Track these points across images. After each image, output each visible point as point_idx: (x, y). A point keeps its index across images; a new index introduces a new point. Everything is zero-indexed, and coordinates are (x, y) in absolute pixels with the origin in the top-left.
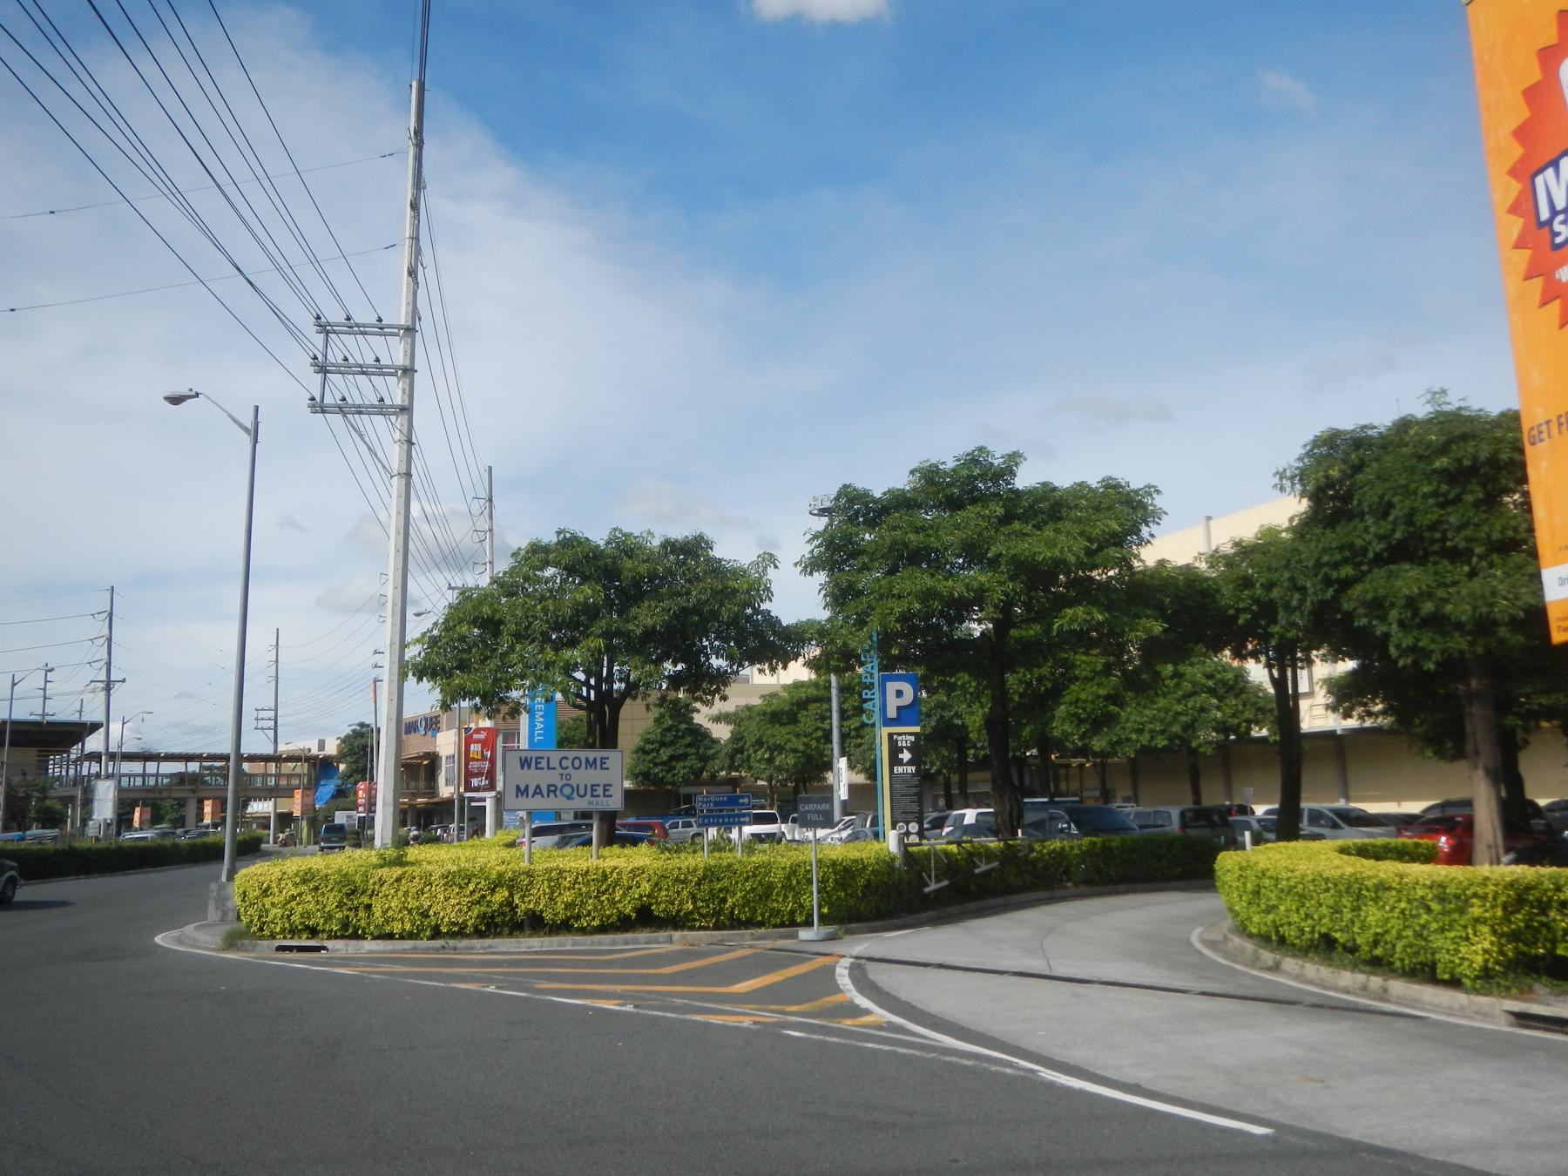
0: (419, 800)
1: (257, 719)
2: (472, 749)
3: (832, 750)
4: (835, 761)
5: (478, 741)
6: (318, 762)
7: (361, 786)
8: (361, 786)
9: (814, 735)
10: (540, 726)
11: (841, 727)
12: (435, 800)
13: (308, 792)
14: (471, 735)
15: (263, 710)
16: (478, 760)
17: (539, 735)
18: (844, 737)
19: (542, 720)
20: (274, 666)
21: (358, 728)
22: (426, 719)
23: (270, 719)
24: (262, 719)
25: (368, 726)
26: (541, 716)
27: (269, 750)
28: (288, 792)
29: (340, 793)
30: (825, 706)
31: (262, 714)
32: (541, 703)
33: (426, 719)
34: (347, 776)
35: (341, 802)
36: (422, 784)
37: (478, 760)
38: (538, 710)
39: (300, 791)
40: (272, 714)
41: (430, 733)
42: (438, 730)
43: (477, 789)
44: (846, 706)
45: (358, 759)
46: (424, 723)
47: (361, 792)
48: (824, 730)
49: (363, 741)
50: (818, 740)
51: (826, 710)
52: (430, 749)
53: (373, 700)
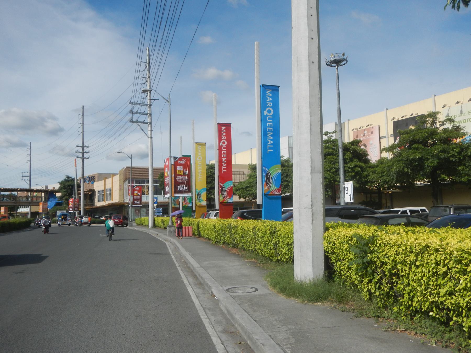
0: (87, 207)
1: (22, 176)
2: (178, 169)
3: (340, 178)
4: (341, 183)
5: (181, 165)
6: (48, 192)
7: (71, 200)
8: (71, 200)
9: (332, 171)
10: (270, 142)
11: (344, 167)
12: (94, 207)
13: (45, 204)
14: (177, 161)
15: (25, 173)
16: (181, 175)
17: (270, 148)
18: (345, 172)
19: (272, 138)
20: (29, 157)
21: (67, 178)
22: (89, 178)
23: (28, 176)
24: (25, 176)
25: (71, 177)
26: (271, 135)
27: (27, 187)
28: (37, 204)
29: (58, 204)
30: (335, 157)
31: (24, 175)
32: (271, 127)
33: (89, 178)
34: (61, 198)
35: (59, 207)
36: (88, 201)
37: (181, 175)
38: (269, 131)
39: (42, 203)
40: (29, 174)
41: (91, 183)
42: (94, 181)
43: (181, 192)
44: (346, 157)
45: (67, 190)
46: (88, 179)
47: (70, 203)
48: (335, 168)
49: (69, 183)
50: (333, 173)
51: (336, 159)
52: (92, 188)
53: (75, 166)
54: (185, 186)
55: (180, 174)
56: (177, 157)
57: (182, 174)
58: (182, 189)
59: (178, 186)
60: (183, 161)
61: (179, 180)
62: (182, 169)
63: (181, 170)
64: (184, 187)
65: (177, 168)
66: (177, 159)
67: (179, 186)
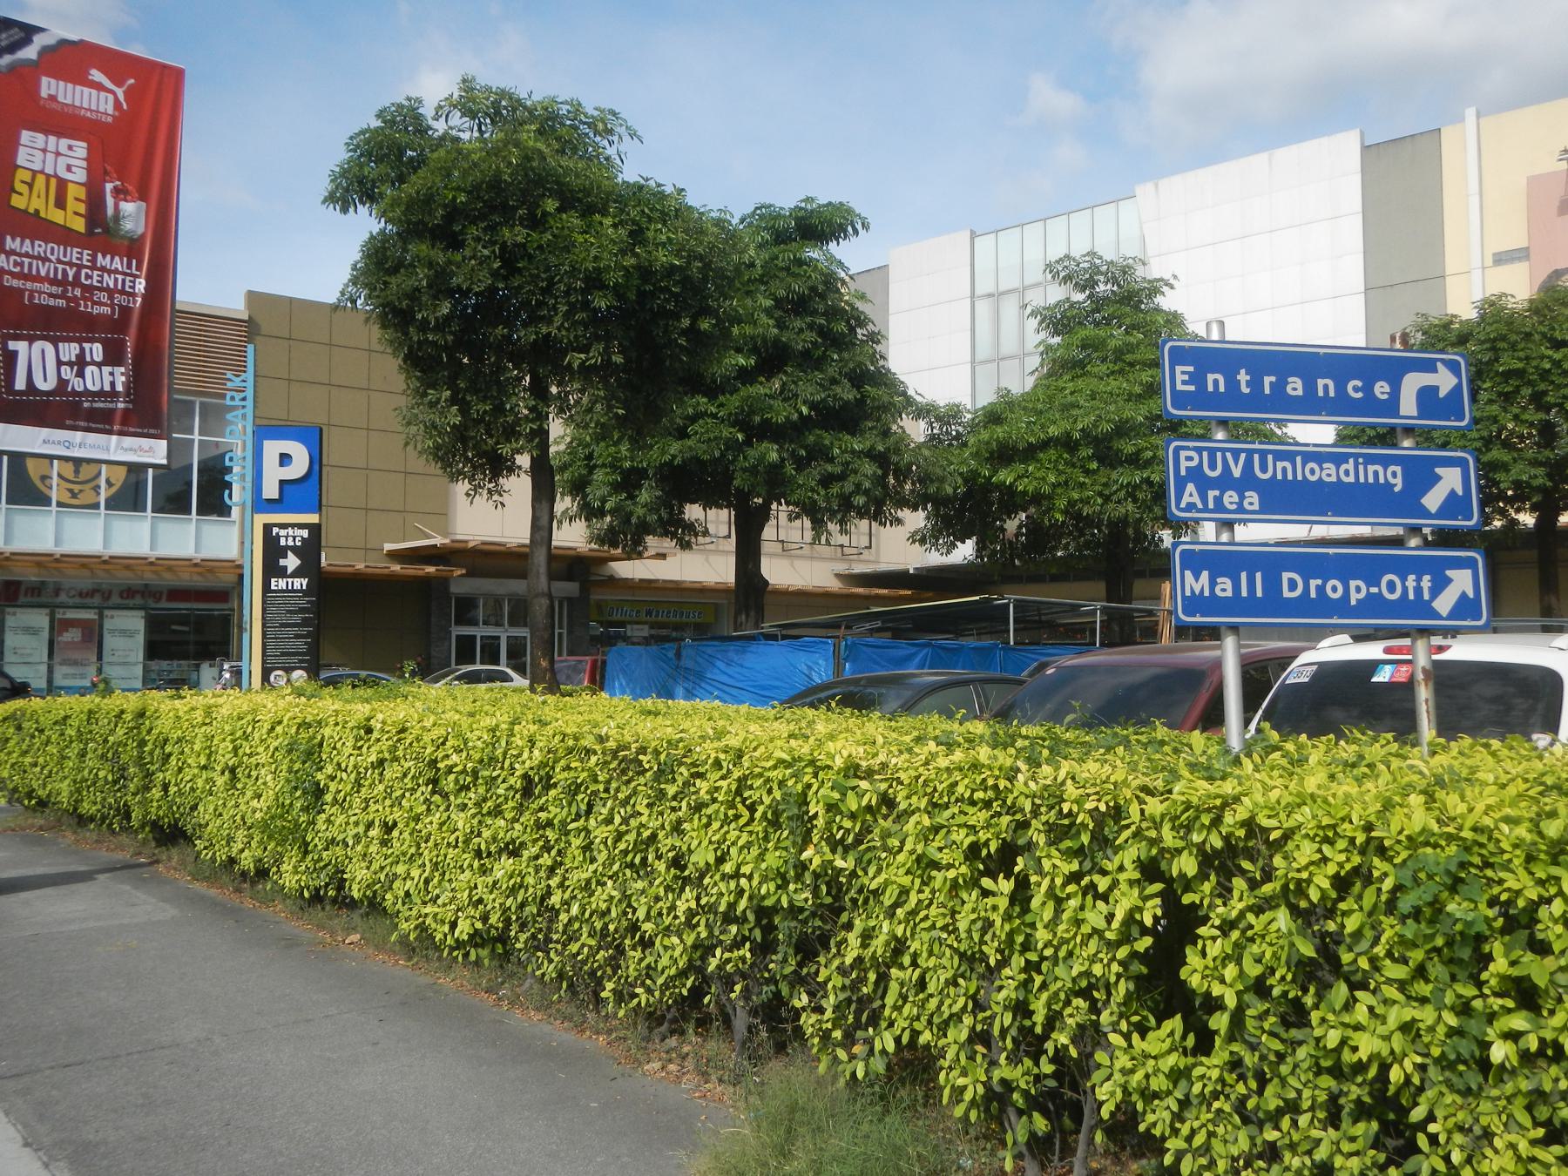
16: (64, 236)
37: (64, 236)
54: (98, 357)
55: (57, 216)
56: (28, 32)
57: (79, 225)
58: (63, 383)
59: (20, 346)
60: (99, 87)
61: (38, 278)
62: (80, 175)
63: (62, 184)
64: (80, 364)
65: (14, 144)
66: (30, 53)
67: (31, 340)
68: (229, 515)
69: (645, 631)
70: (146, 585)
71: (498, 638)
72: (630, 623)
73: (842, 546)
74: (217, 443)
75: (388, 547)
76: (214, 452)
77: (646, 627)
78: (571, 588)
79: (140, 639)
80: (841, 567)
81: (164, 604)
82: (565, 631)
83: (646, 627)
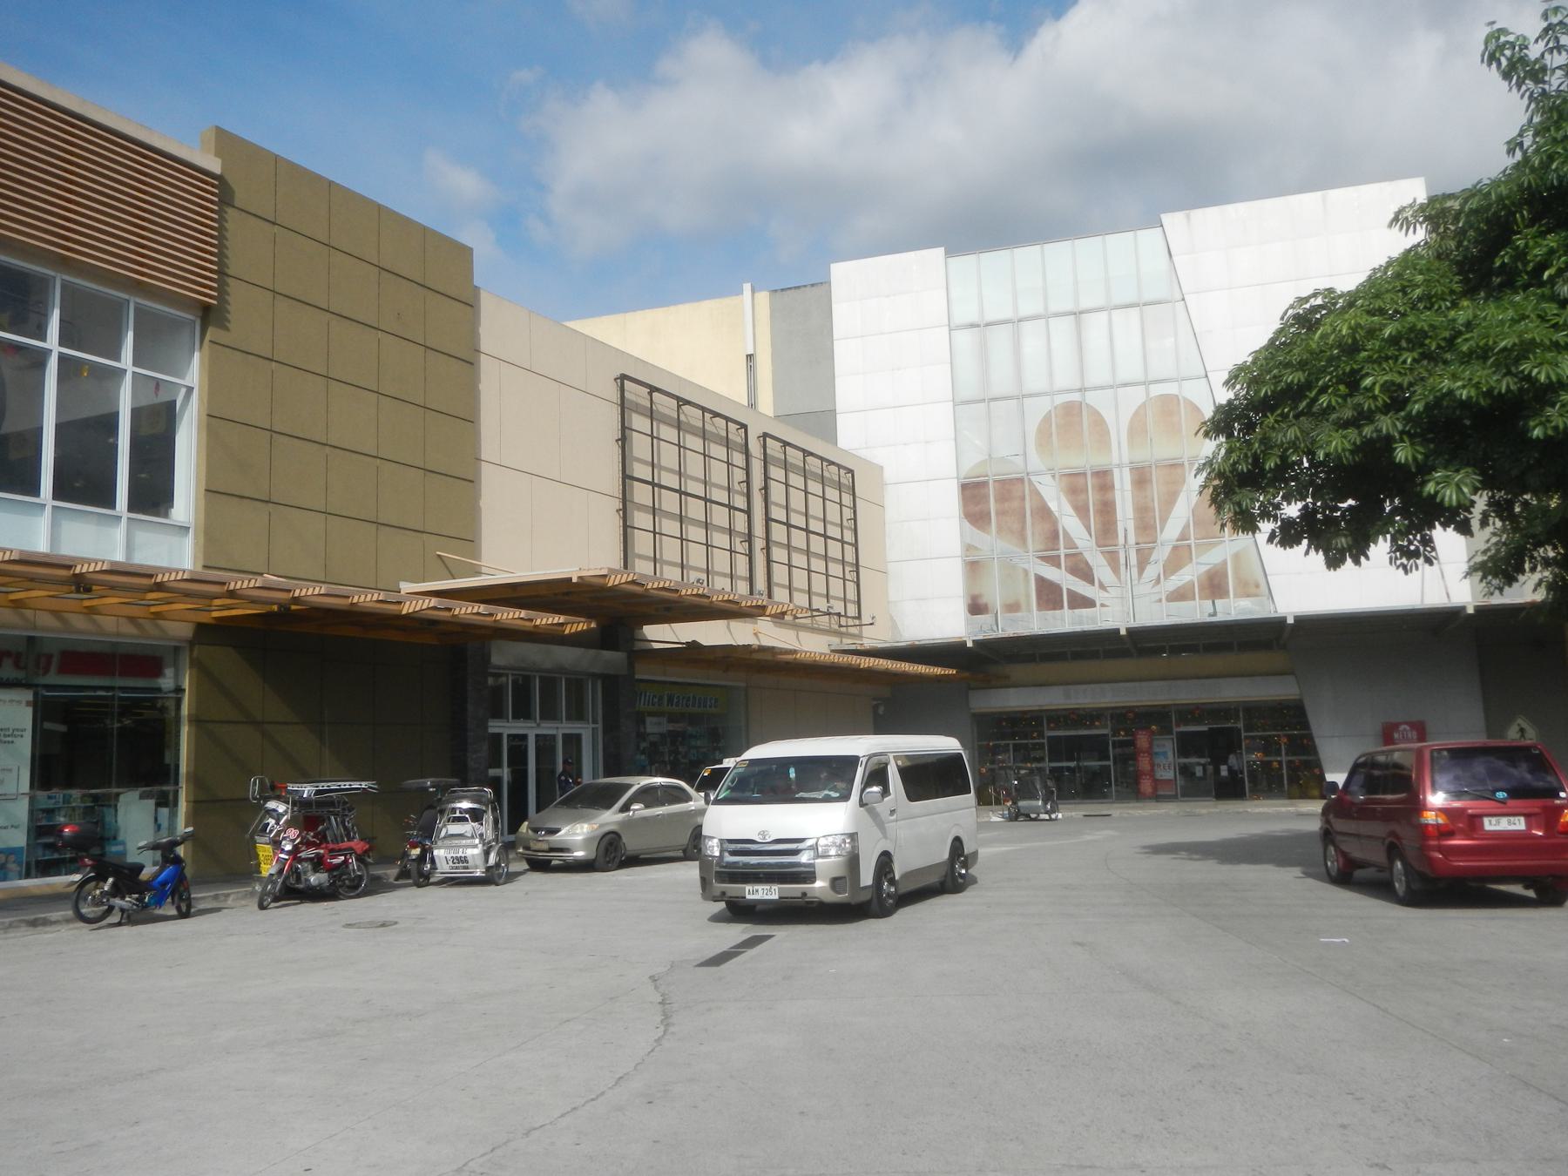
68: (166, 515)
69: (666, 727)
70: (31, 639)
71: (524, 737)
72: (651, 714)
73: (839, 615)
74: (158, 382)
75: (406, 587)
76: (149, 399)
77: (664, 720)
78: (612, 659)
79: (25, 745)
80: (835, 642)
81: (53, 678)
82: (600, 726)
83: (664, 720)
